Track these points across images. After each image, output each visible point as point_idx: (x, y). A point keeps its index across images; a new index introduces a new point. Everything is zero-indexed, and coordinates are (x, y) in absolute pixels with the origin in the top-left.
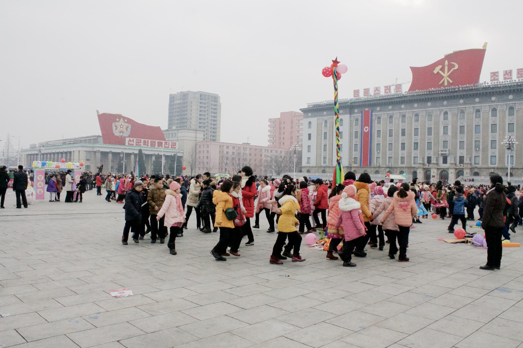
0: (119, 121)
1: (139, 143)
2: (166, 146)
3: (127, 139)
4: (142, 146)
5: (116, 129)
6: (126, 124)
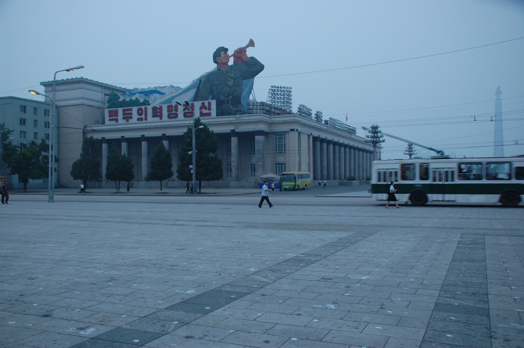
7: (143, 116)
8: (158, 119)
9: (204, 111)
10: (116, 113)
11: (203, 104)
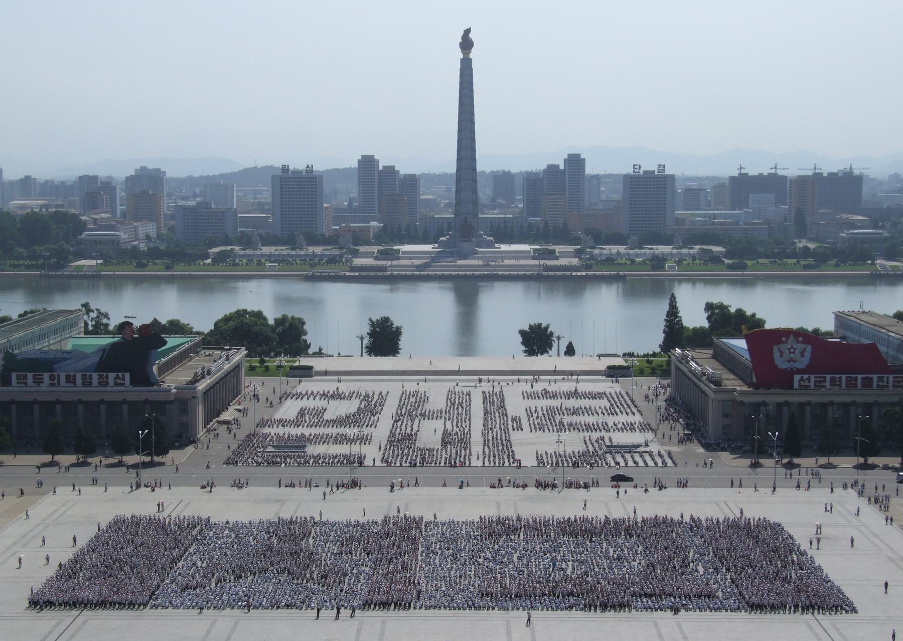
0: (786, 342)
1: (820, 382)
2: (881, 383)
3: (797, 378)
4: (828, 387)
5: (781, 356)
7: (56, 381)
8: (72, 385)
9: (118, 381)
10: (26, 377)
11: (118, 375)
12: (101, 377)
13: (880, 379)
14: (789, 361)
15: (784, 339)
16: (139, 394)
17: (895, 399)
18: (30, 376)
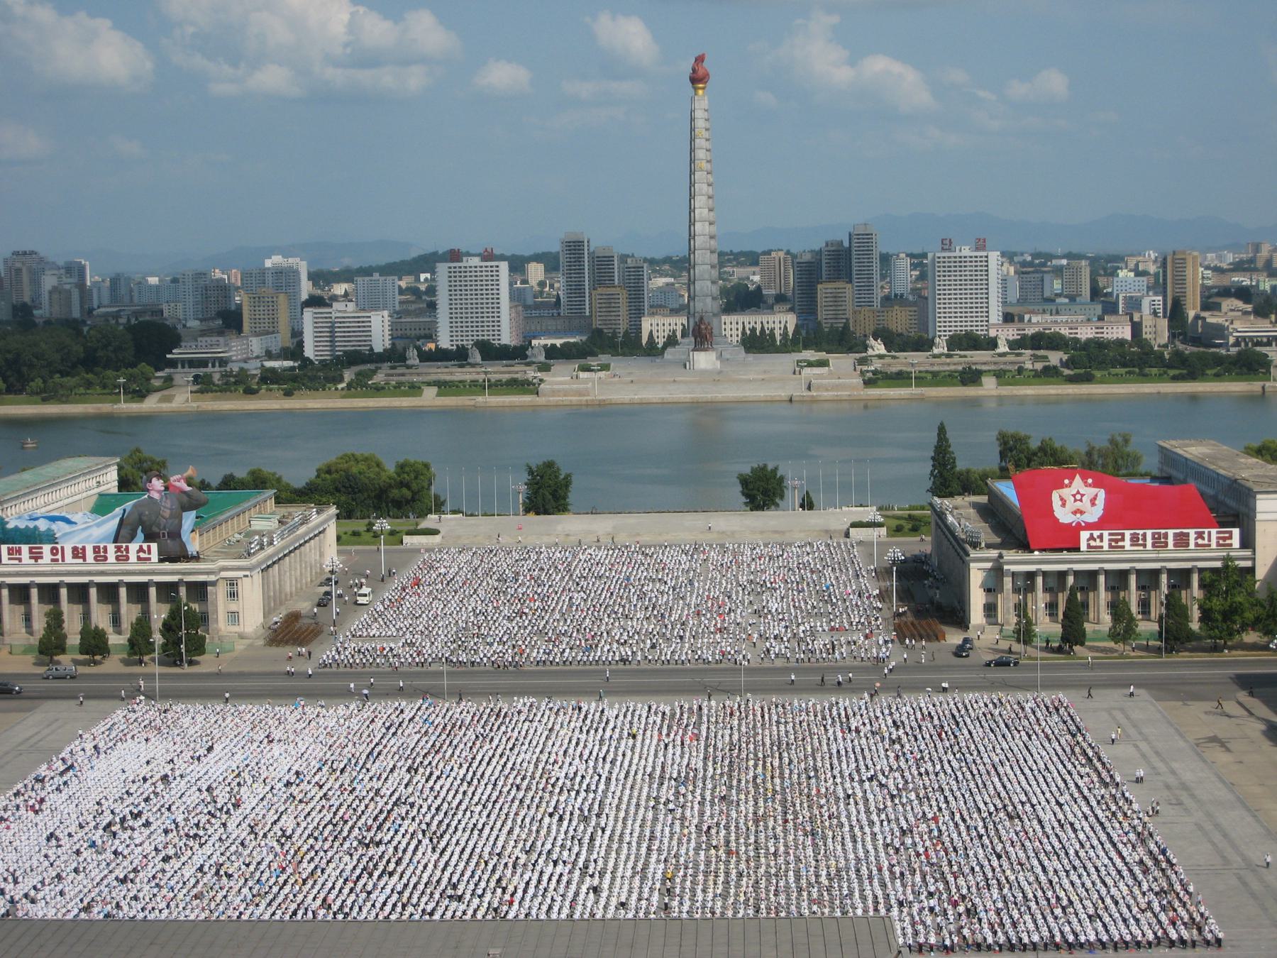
1: (1117, 541)
2: (1200, 541)
3: (1084, 535)
4: (1128, 547)
5: (1064, 505)
6: (1093, 491)
7: (59, 557)
8: (81, 561)
9: (142, 555)
10: (19, 552)
12: (119, 549)
13: (1200, 536)
14: (1075, 513)
15: (1066, 481)
16: (170, 573)
17: (1218, 564)
18: (25, 548)
